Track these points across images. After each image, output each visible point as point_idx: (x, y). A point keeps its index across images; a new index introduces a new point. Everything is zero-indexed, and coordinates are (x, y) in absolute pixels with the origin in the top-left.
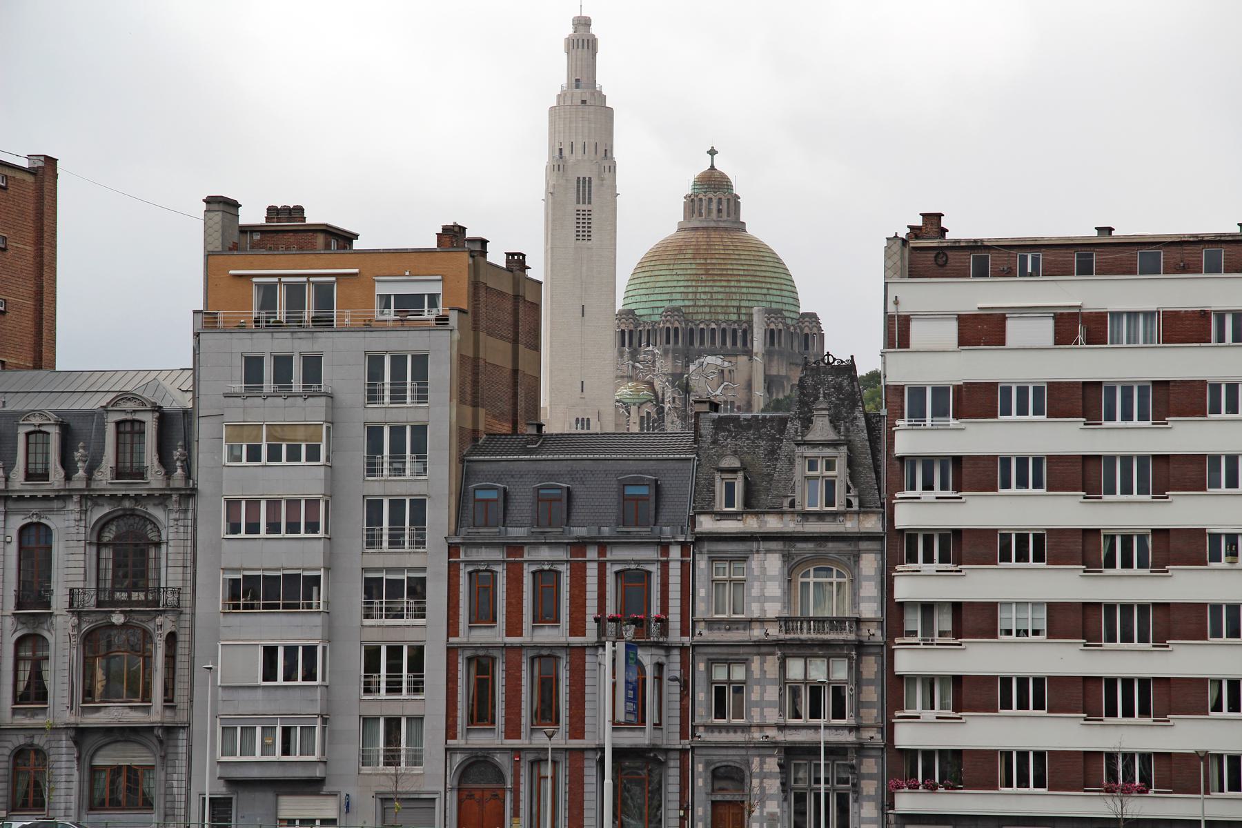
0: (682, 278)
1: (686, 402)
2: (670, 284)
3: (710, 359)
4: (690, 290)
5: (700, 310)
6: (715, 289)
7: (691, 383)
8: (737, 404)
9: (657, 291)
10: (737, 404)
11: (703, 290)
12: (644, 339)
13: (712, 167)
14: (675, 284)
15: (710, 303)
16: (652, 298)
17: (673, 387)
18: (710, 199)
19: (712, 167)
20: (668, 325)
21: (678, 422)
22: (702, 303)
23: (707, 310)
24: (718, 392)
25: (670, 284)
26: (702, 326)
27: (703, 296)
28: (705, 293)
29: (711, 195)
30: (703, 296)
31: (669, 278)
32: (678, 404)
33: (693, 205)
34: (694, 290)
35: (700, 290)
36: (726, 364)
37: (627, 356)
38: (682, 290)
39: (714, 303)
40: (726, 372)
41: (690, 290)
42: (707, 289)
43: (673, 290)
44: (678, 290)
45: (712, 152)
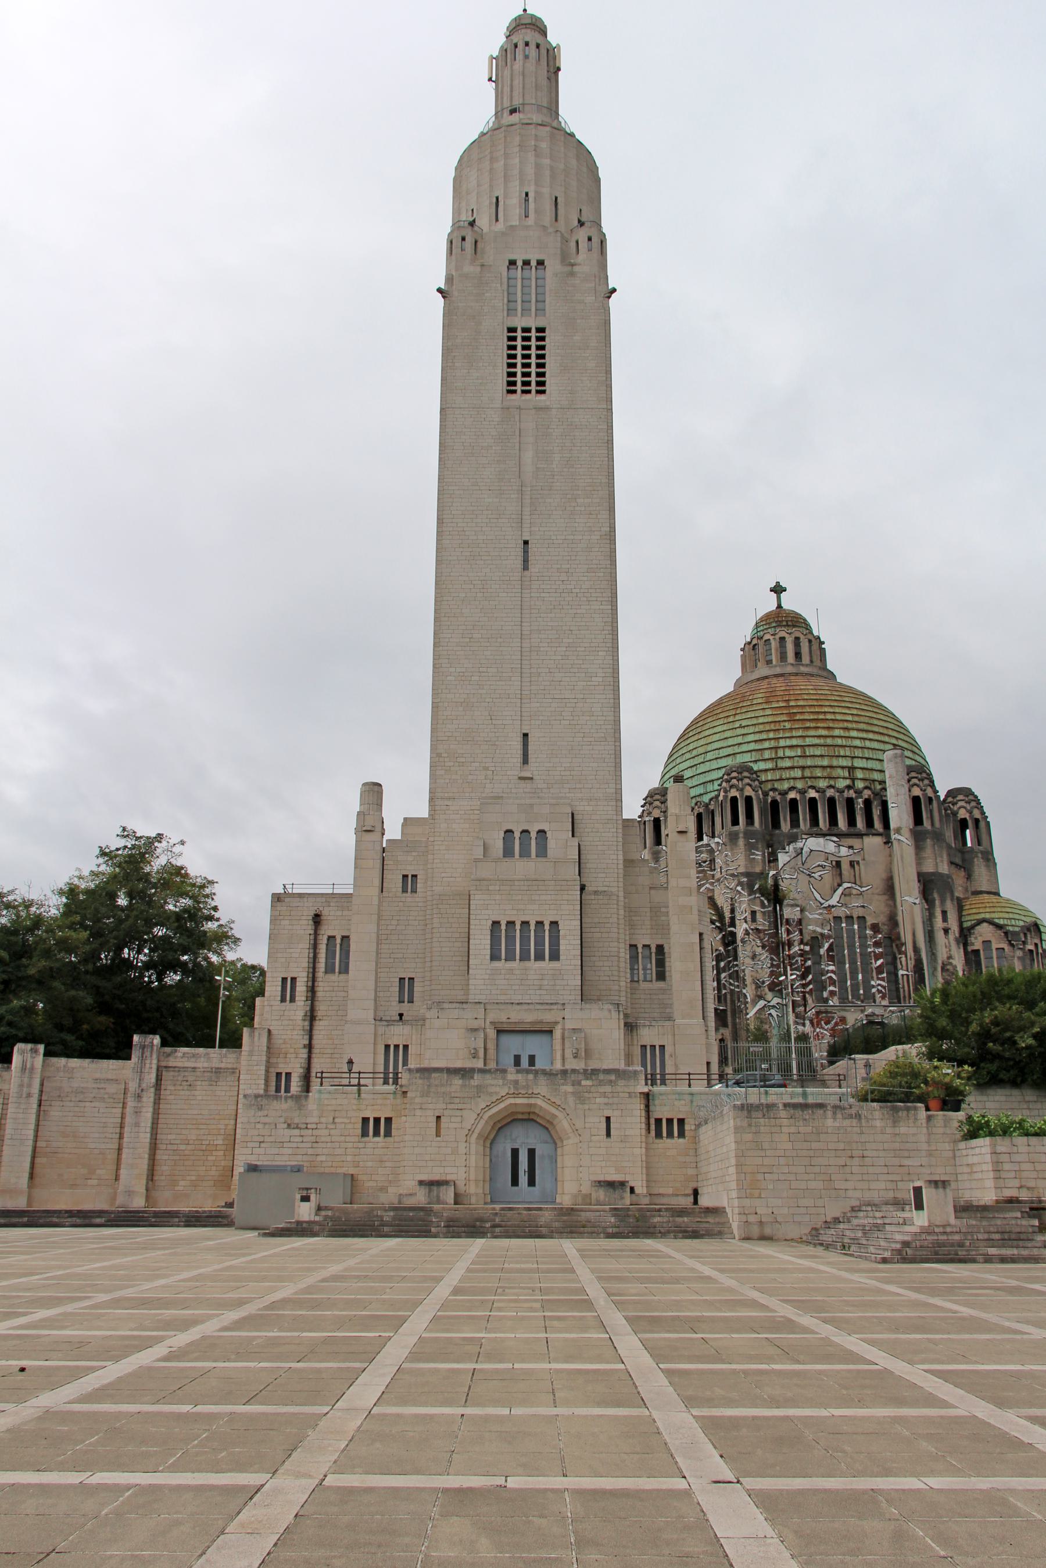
0: (751, 730)
1: (776, 920)
3: (813, 843)
4: (766, 745)
5: (786, 774)
7: (783, 885)
8: (870, 921)
9: (710, 756)
10: (870, 921)
11: (788, 742)
13: (779, 606)
14: (740, 740)
15: (802, 762)
16: (702, 768)
17: (751, 892)
18: (782, 639)
19: (779, 606)
20: (734, 793)
21: (764, 955)
22: (788, 763)
23: (798, 773)
24: (833, 901)
25: (730, 742)
26: (792, 795)
27: (789, 753)
28: (791, 747)
29: (782, 634)
30: (788, 753)
31: (728, 734)
32: (762, 923)
34: (773, 744)
35: (782, 743)
36: (844, 851)
38: (752, 746)
39: (809, 762)
40: (845, 866)
41: (766, 745)
42: (794, 742)
43: (737, 749)
44: (745, 748)
45: (778, 590)
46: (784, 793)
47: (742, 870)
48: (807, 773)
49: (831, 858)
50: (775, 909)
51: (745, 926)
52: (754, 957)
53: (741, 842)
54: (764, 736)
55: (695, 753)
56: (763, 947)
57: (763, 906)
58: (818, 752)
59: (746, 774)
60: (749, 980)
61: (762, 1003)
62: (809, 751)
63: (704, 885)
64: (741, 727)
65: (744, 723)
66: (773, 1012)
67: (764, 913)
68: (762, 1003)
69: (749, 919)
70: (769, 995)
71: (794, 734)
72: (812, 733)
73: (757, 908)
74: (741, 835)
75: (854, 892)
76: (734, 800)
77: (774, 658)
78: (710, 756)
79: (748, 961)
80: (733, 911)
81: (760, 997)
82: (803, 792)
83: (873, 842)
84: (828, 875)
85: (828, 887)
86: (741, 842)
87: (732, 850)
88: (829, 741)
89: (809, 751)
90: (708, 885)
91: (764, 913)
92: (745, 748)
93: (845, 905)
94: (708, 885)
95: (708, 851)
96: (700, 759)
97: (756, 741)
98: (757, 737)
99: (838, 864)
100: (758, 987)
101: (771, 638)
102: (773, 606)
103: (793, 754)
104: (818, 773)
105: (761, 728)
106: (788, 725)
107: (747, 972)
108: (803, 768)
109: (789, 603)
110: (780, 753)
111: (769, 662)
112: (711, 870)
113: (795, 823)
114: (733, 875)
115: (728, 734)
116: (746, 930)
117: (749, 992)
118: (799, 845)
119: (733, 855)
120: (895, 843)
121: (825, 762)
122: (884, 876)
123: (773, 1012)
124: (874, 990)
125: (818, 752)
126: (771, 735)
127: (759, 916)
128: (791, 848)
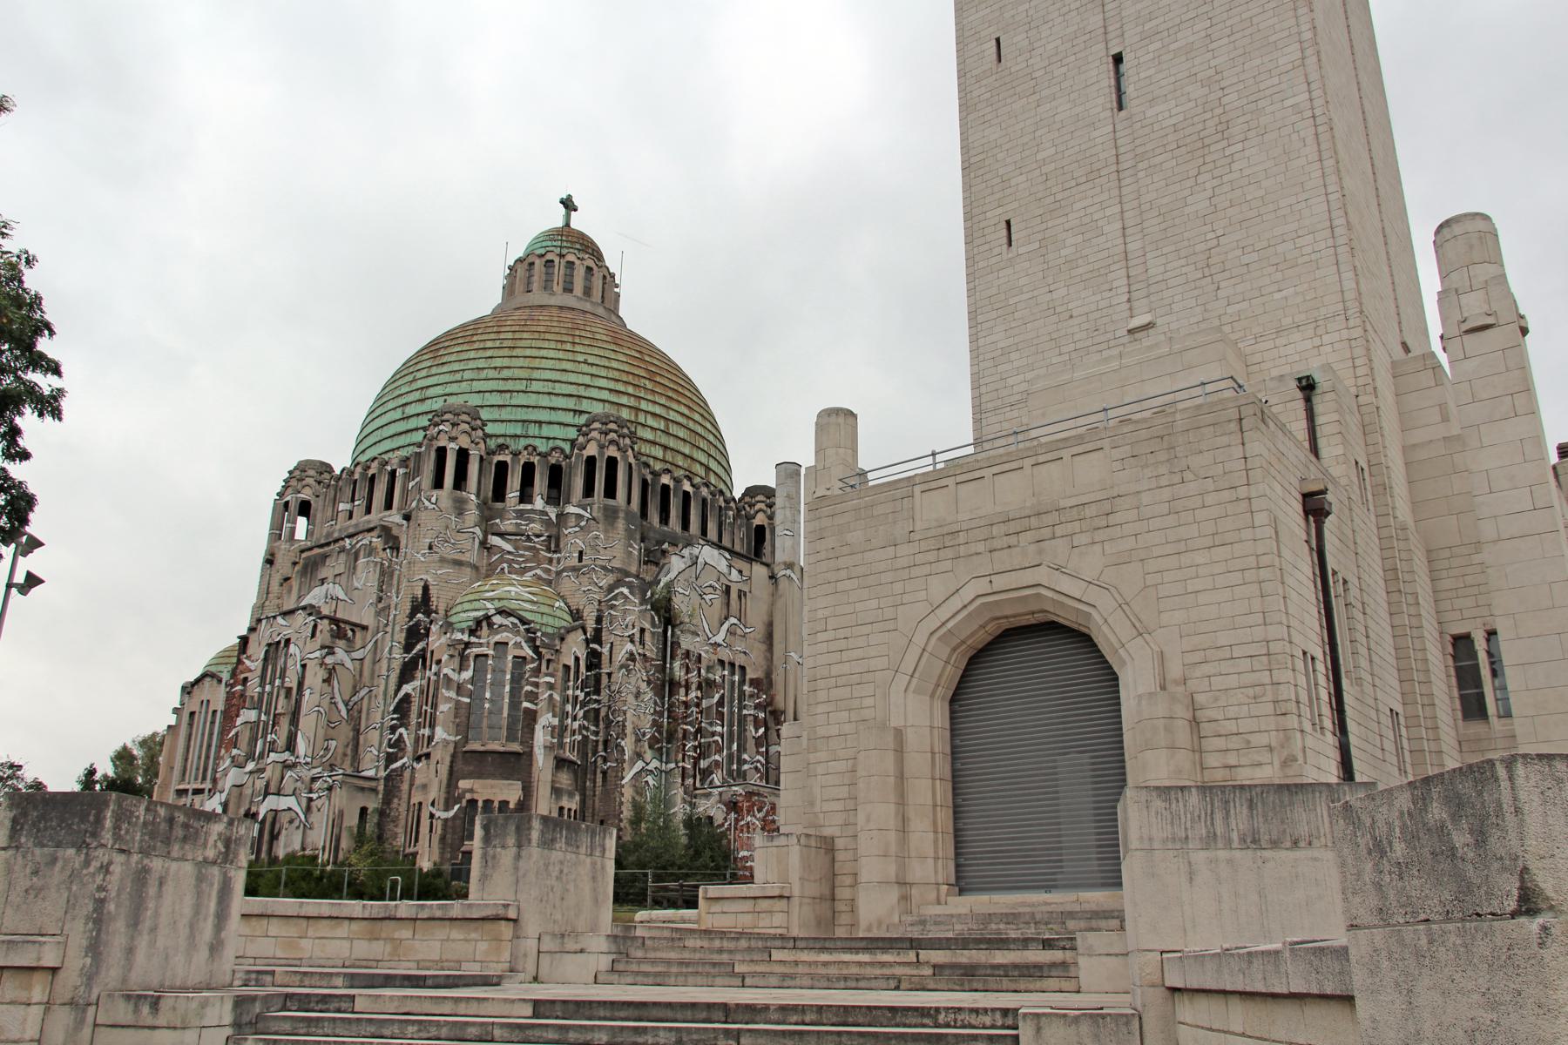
0: (603, 373)
1: (668, 648)
2: (572, 378)
3: (708, 554)
4: (624, 400)
6: (672, 415)
7: (677, 601)
9: (536, 386)
10: (750, 675)
11: (651, 408)
12: (514, 482)
13: (568, 225)
14: (587, 380)
15: (664, 440)
17: (643, 601)
20: (612, 451)
21: (649, 695)
22: (648, 435)
23: (659, 452)
24: (719, 639)
25: (572, 378)
26: (665, 480)
27: (651, 422)
28: (654, 415)
30: (651, 422)
31: (568, 366)
32: (651, 649)
33: (523, 273)
34: (632, 402)
35: (644, 405)
36: (735, 575)
37: (472, 514)
38: (605, 395)
39: (672, 443)
40: (734, 595)
41: (624, 400)
42: (658, 410)
43: (582, 391)
44: (594, 393)
45: (568, 204)
46: (656, 475)
47: (617, 564)
48: (669, 457)
49: (723, 580)
50: (665, 632)
51: (629, 646)
52: (638, 695)
53: (621, 524)
54: (621, 387)
55: (506, 373)
56: (649, 682)
57: (653, 625)
58: (682, 433)
59: (612, 426)
60: (629, 730)
61: (640, 764)
62: (673, 429)
63: (531, 569)
64: (585, 362)
65: (591, 360)
66: (649, 779)
67: (653, 634)
68: (640, 764)
69: (637, 638)
70: (649, 755)
71: (657, 399)
72: (675, 406)
73: (647, 626)
74: (622, 515)
75: (739, 632)
76: (442, 452)
77: (535, 286)
78: (536, 386)
79: (631, 699)
80: (599, 620)
81: (639, 756)
82: (656, 475)
83: (759, 571)
84: (715, 598)
85: (716, 617)
86: (621, 524)
87: (606, 531)
88: (691, 425)
89: (673, 429)
90: (538, 572)
91: (653, 634)
92: (594, 393)
93: (729, 646)
94: (538, 572)
95: (542, 521)
96: (521, 386)
97: (611, 390)
98: (612, 385)
99: (728, 590)
100: (638, 740)
101: (557, 260)
102: (560, 223)
103: (655, 425)
104: (680, 461)
105: (616, 375)
106: (649, 385)
107: (628, 715)
108: (665, 448)
109: (577, 222)
110: (641, 419)
111: (568, 289)
112: (549, 550)
113: (665, 519)
114: (604, 568)
115: (568, 366)
116: (632, 654)
117: (628, 744)
118: (696, 551)
119: (607, 538)
120: (783, 584)
121: (687, 450)
122: (766, 618)
123: (649, 779)
124: (746, 767)
125: (682, 433)
126: (630, 390)
127: (647, 636)
128: (686, 552)
